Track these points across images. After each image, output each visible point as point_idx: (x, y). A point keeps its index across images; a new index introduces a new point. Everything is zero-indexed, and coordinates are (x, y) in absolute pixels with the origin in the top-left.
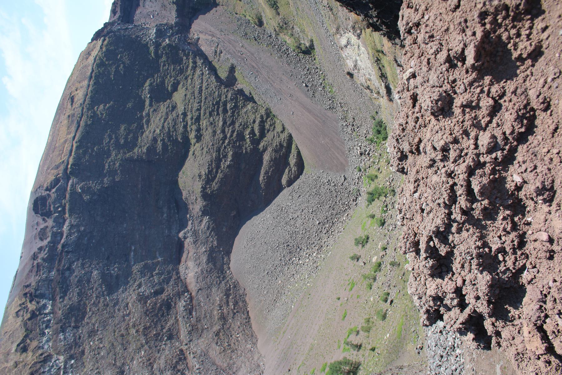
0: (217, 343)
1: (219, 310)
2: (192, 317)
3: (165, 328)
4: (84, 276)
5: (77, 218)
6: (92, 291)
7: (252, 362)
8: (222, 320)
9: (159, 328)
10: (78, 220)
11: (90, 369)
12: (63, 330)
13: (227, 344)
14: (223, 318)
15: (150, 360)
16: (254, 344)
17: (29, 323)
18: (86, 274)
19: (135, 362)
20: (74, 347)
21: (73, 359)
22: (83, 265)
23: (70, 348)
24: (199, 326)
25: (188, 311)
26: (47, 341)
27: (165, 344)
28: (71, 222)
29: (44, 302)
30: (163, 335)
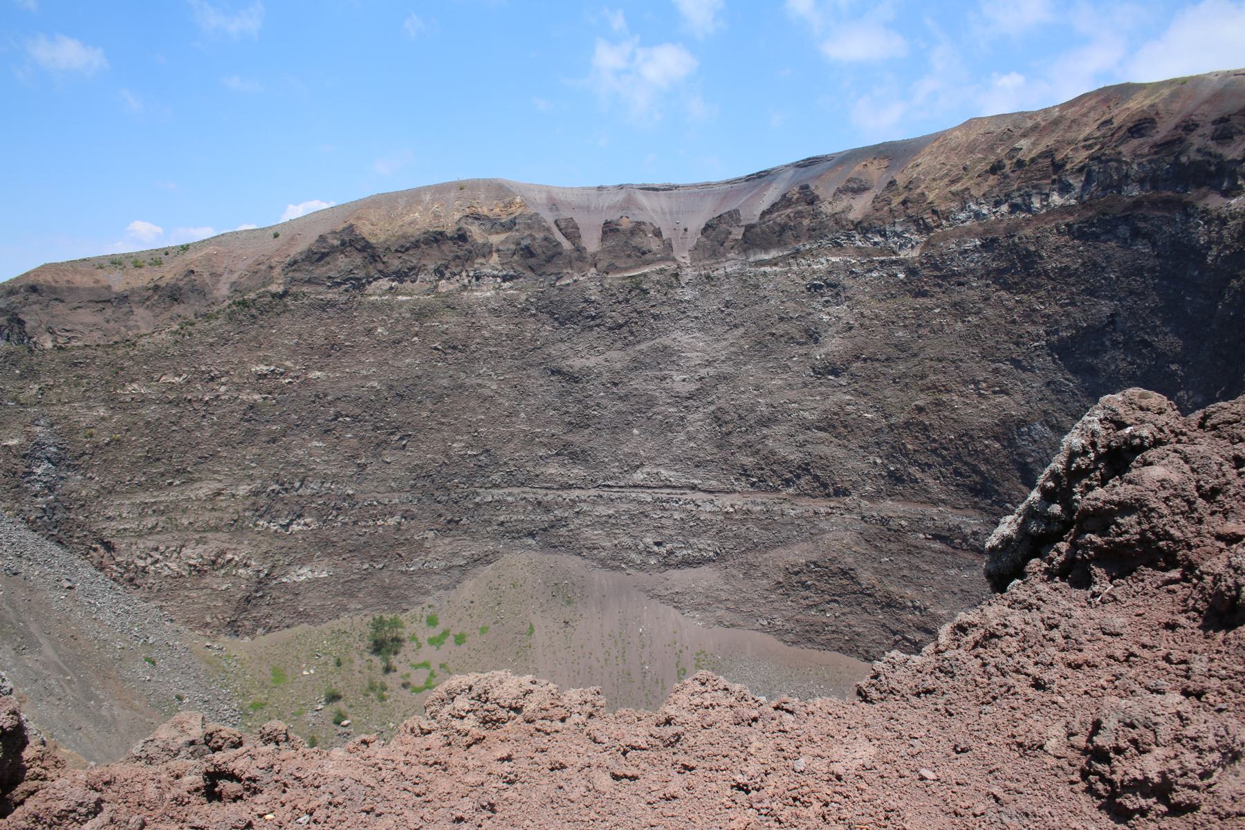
0: (815, 563)
1: (912, 602)
2: (926, 538)
3: (923, 471)
4: (1105, 279)
5: (1232, 237)
6: (1067, 304)
7: (720, 602)
8: (884, 599)
9: (922, 458)
10: (1229, 241)
11: (867, 312)
12: (989, 244)
13: (809, 583)
14: (890, 604)
15: (845, 427)
16: (779, 633)
17: (1047, 162)
18: (1110, 285)
19: (848, 397)
20: (938, 274)
21: (906, 277)
22: (1138, 271)
23: (936, 267)
24: (892, 546)
25: (948, 534)
26: (977, 215)
27: (875, 463)
28: (1234, 218)
29: (1076, 185)
30: (902, 463)
